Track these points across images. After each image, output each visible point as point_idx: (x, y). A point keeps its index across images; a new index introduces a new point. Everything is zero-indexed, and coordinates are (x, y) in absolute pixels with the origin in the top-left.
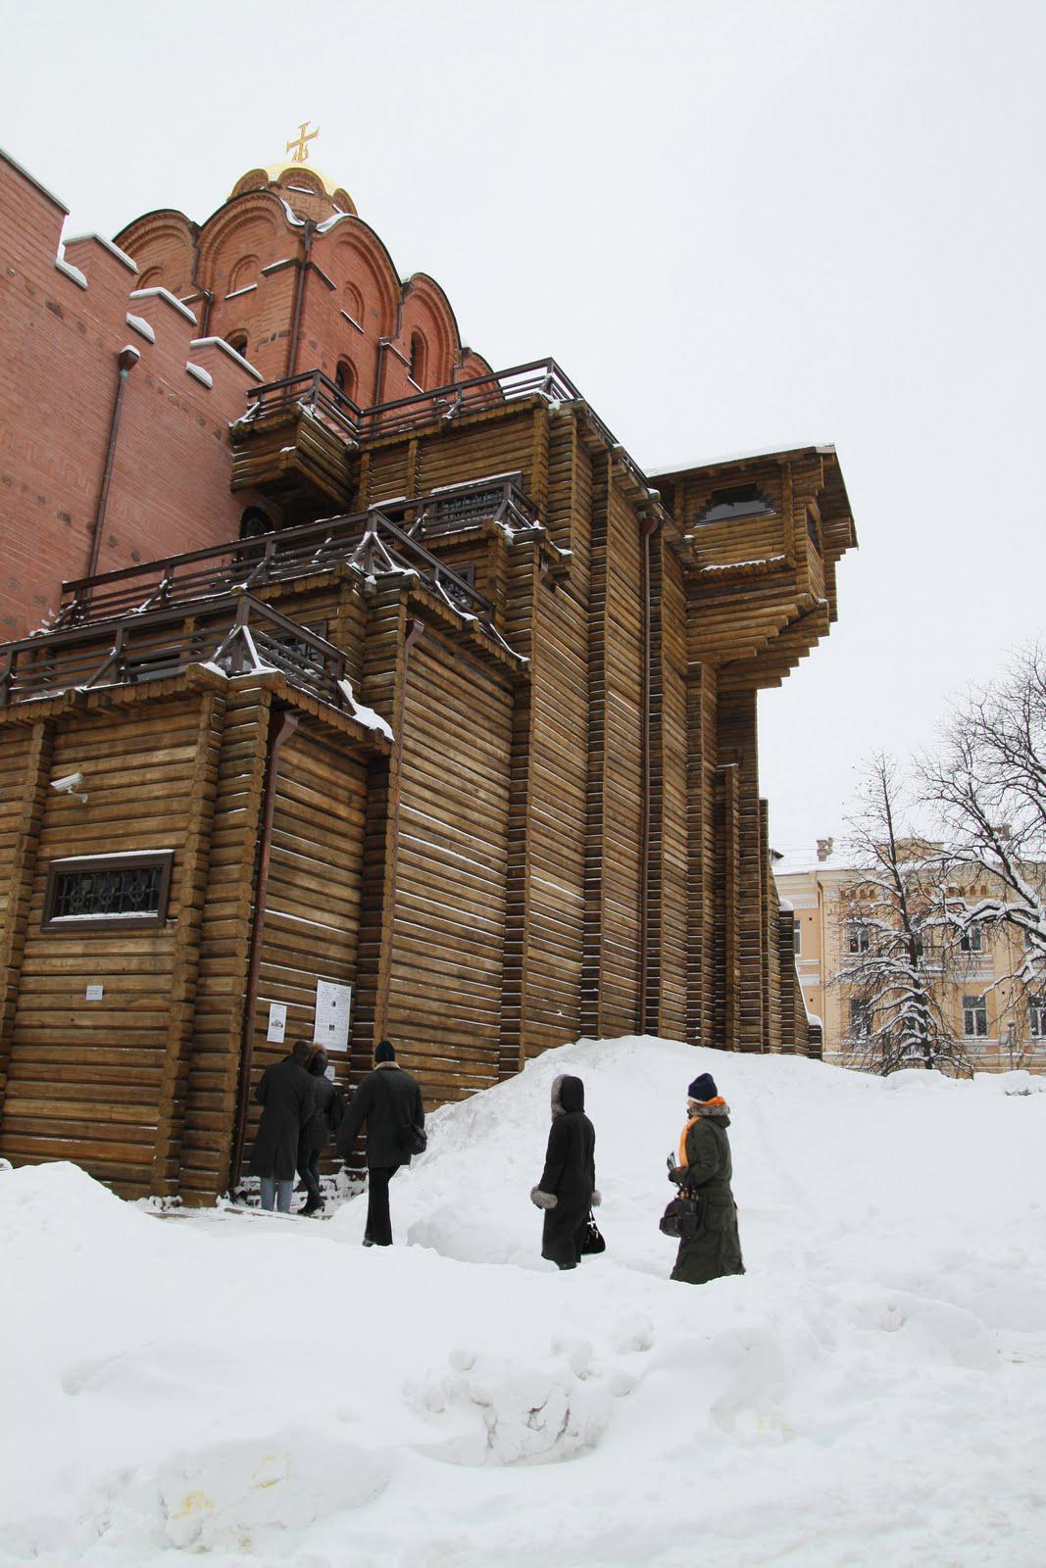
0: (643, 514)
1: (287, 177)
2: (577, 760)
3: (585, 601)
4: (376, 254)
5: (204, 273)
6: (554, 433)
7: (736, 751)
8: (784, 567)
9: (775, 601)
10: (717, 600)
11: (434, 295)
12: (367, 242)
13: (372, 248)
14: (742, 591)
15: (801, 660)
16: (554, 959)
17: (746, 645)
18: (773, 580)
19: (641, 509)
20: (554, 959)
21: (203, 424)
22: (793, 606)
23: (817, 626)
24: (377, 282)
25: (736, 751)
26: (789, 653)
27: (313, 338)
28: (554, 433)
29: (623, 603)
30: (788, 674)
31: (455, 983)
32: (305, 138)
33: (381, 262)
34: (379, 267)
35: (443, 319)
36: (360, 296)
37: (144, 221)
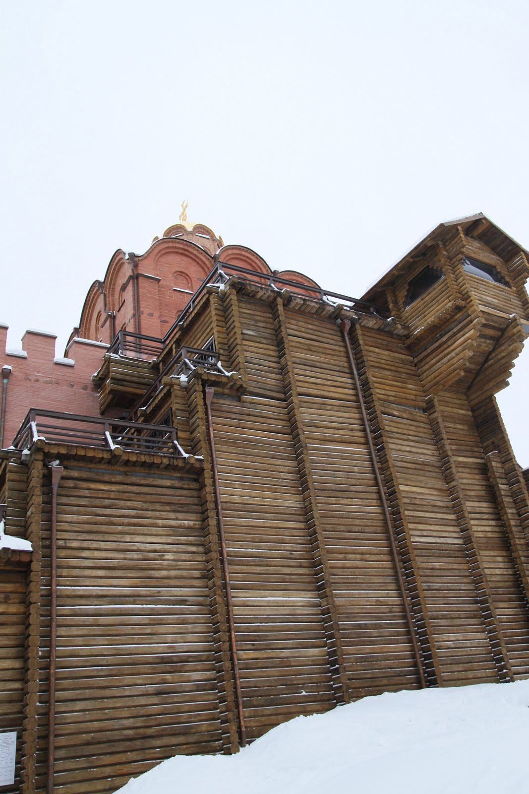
0: (339, 321)
1: (197, 227)
2: (291, 502)
3: (282, 396)
4: (190, 249)
5: (109, 304)
6: (225, 304)
7: (493, 443)
8: (458, 309)
9: (461, 333)
10: (429, 350)
11: (244, 253)
12: (182, 246)
13: (187, 248)
14: (442, 336)
15: (514, 361)
16: (286, 653)
17: (455, 370)
18: (456, 320)
19: (336, 318)
20: (286, 653)
21: (72, 386)
22: (472, 331)
23: (514, 334)
24: (198, 263)
25: (493, 443)
26: (504, 361)
27: (150, 311)
28: (225, 304)
29: (329, 383)
30: (510, 375)
31: (155, 699)
32: (184, 210)
33: (195, 252)
34: (195, 255)
35: (255, 263)
36: (187, 275)
37: (91, 292)
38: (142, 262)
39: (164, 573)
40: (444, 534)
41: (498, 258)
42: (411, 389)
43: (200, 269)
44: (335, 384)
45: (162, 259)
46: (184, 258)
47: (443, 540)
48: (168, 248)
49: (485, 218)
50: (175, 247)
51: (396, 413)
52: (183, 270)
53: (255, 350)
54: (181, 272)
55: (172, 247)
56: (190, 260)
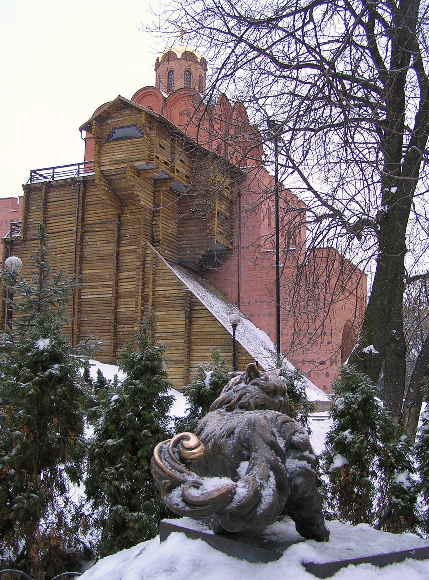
44: (69, 222)
47: (103, 296)
51: (97, 230)
53: (35, 216)
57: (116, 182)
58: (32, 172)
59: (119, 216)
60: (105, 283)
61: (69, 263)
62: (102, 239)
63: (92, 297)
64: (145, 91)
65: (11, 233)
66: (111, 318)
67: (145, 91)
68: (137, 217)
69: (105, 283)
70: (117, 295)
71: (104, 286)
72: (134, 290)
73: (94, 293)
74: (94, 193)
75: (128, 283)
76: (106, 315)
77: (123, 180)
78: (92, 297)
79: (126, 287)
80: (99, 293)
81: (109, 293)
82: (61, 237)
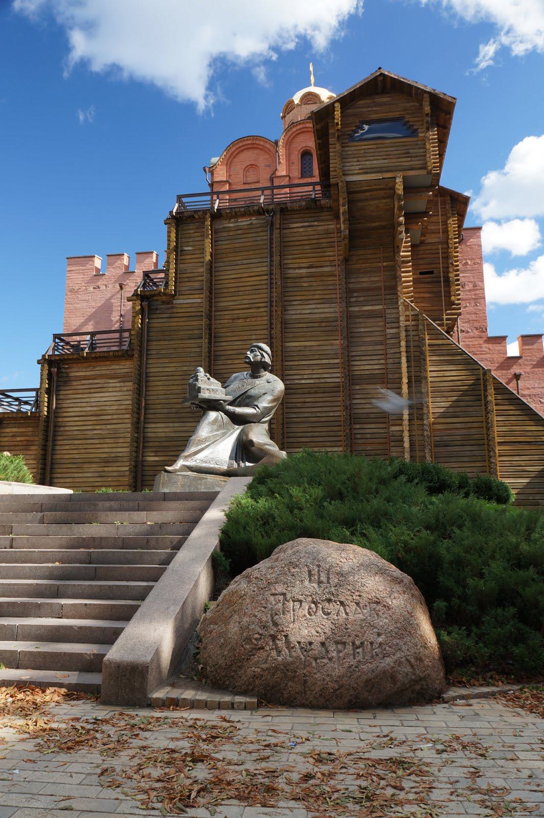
4: (257, 142)
12: (250, 142)
38: (217, 170)
39: (110, 417)
40: (325, 376)
41: (412, 104)
42: (329, 256)
43: (268, 156)
45: (236, 160)
46: (256, 151)
47: (322, 381)
48: (240, 147)
49: (382, 74)
50: (245, 145)
52: (252, 163)
54: (251, 165)
55: (243, 146)
56: (259, 151)
57: (360, 204)
58: (179, 198)
59: (346, 260)
60: (324, 362)
61: (259, 332)
62: (317, 297)
63: (303, 382)
64: (301, 126)
65: (144, 286)
66: (338, 413)
67: (301, 126)
68: (374, 265)
69: (324, 362)
70: (351, 380)
71: (324, 367)
72: (377, 372)
73: (305, 377)
74: (296, 230)
75: (365, 363)
76: (328, 409)
77: (372, 203)
78: (303, 382)
79: (362, 368)
80: (315, 376)
81: (335, 377)
82: (241, 293)
